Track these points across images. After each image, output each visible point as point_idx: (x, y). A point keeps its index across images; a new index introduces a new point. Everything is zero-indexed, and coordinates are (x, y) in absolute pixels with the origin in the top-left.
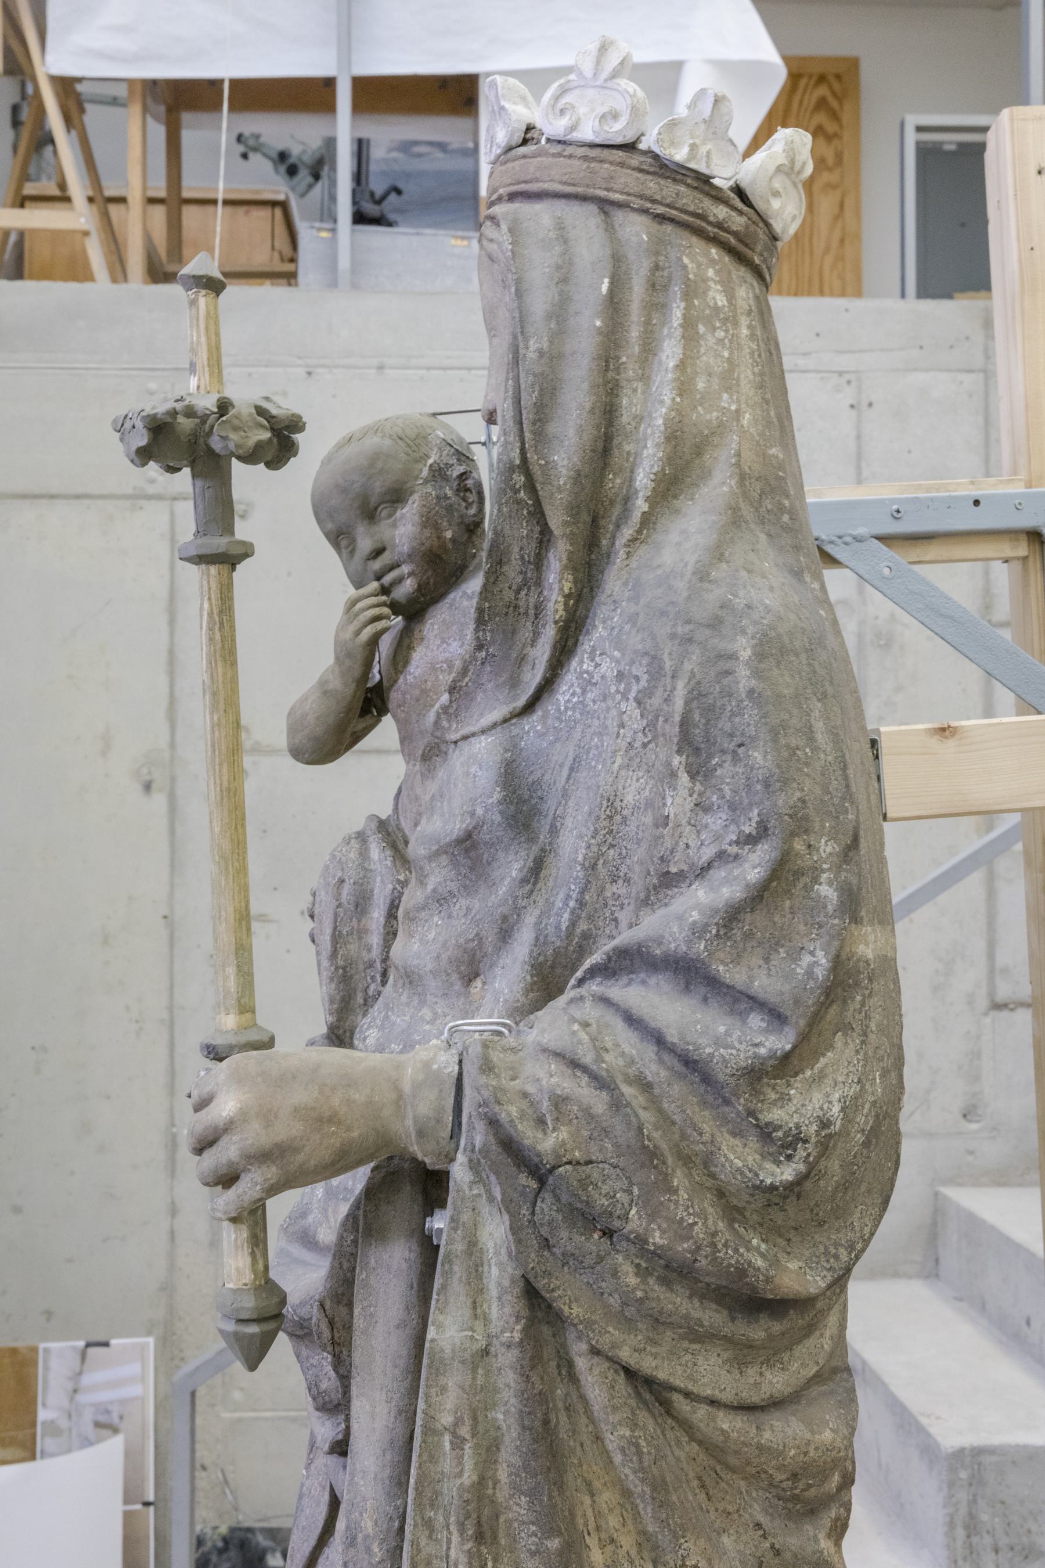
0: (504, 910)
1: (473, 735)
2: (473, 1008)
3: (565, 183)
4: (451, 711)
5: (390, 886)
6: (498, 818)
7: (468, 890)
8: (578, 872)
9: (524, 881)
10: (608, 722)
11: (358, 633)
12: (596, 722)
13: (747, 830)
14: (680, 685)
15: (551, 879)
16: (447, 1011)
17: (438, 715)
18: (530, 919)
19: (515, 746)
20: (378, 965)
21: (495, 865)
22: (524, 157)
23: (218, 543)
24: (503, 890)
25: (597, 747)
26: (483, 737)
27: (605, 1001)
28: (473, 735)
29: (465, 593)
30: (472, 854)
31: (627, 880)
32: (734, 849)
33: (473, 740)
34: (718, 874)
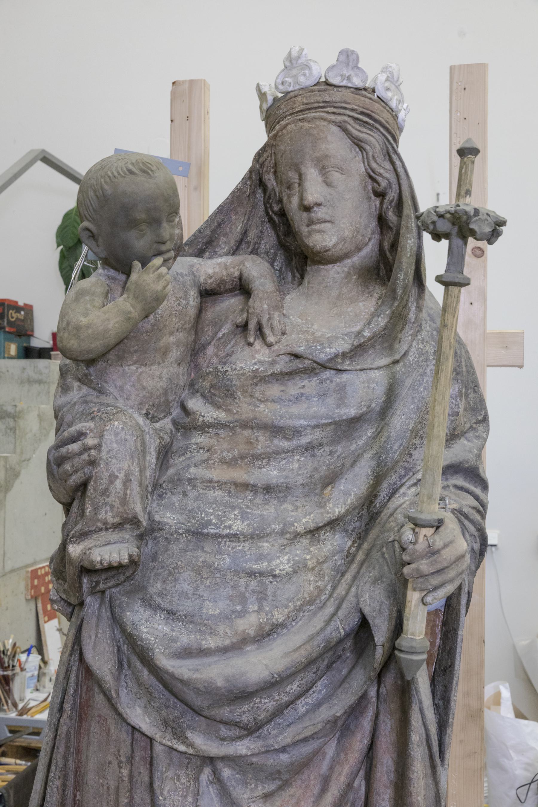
0: (360, 451)
1: (370, 369)
2: (324, 500)
3: (387, 122)
4: (349, 355)
5: (158, 441)
6: (378, 409)
7: (333, 442)
8: (408, 434)
9: (374, 438)
10: (428, 371)
11: (165, 288)
12: (421, 370)
13: (480, 418)
14: (463, 360)
15: (383, 437)
16: (305, 504)
17: (336, 356)
18: (368, 456)
19: (394, 377)
20: (150, 489)
21: (359, 430)
22: (371, 99)
23: (453, 277)
24: (361, 442)
25: (420, 381)
26: (376, 371)
27: (456, 487)
28: (370, 369)
29: (177, 273)
30: (352, 425)
31: (422, 438)
32: (474, 426)
33: (368, 371)
34: (470, 435)
